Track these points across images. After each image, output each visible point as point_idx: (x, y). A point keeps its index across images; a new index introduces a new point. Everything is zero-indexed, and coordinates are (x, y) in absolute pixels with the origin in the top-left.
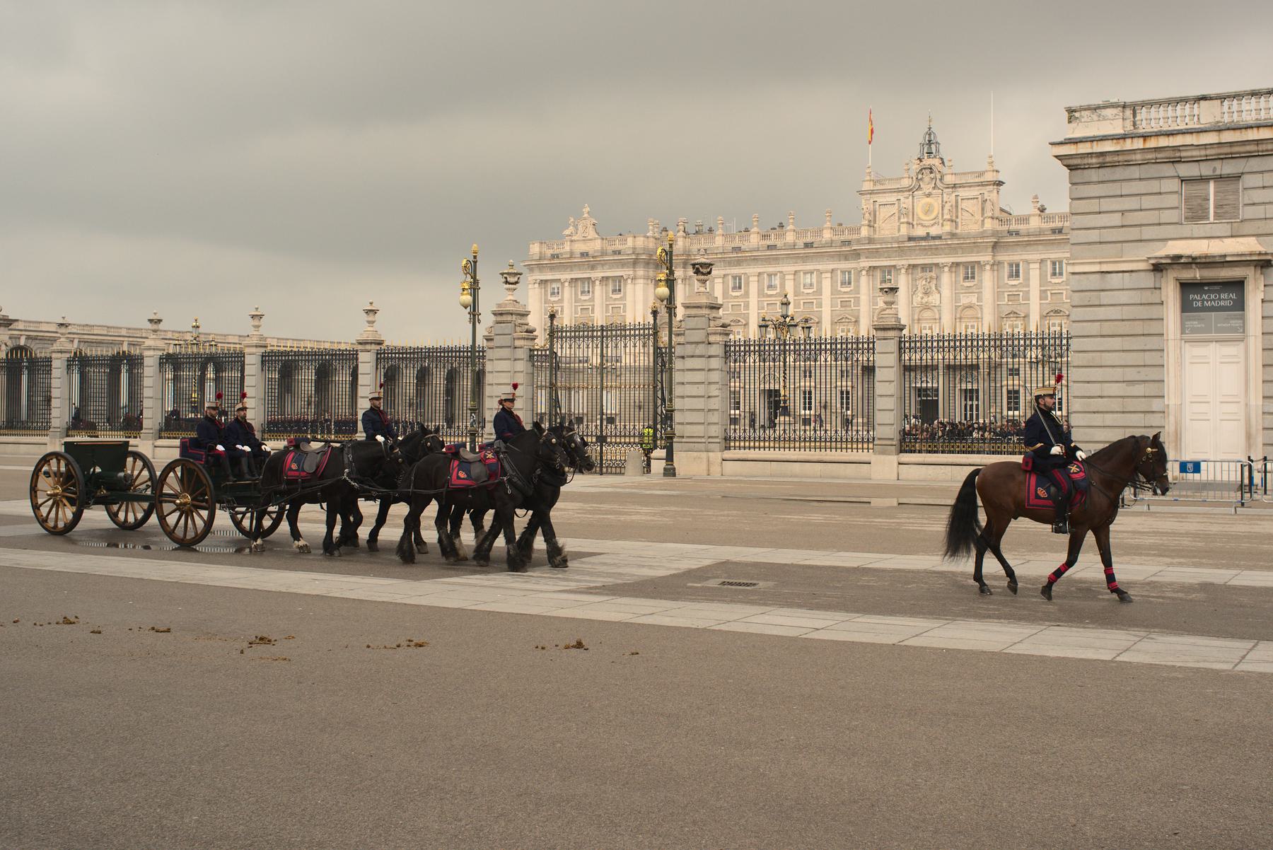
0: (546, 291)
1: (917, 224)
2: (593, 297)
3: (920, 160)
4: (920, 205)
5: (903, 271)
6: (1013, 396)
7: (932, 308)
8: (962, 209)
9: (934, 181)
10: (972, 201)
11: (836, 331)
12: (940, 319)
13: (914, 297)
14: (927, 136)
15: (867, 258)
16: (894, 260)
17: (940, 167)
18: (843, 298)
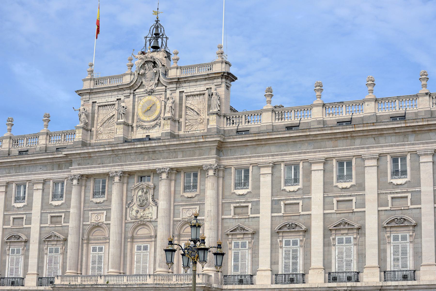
1: (137, 127)
4: (141, 105)
5: (117, 179)
7: (148, 224)
9: (157, 78)
10: (197, 98)
12: (156, 237)
13: (128, 209)
15: (79, 164)
16: (107, 166)
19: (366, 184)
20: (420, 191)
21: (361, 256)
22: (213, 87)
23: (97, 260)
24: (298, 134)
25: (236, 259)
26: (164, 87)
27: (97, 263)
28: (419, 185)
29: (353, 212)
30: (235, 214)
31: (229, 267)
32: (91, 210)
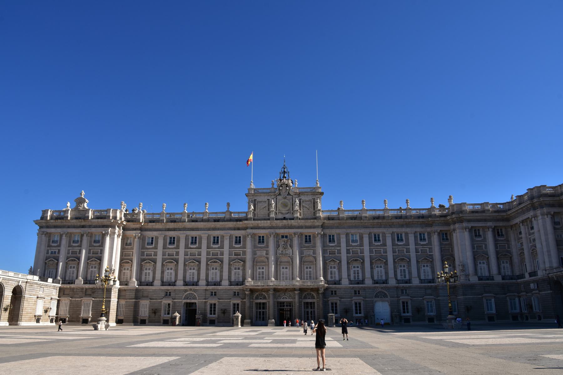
0: (49, 240)
2: (81, 244)
3: (281, 180)
6: (334, 305)
8: (303, 206)
9: (288, 192)
11: (231, 268)
13: (277, 250)
14: (283, 169)
15: (252, 229)
17: (291, 184)
18: (235, 251)
19: (387, 244)
20: (409, 248)
21: (387, 273)
22: (316, 198)
23: (261, 273)
24: (358, 222)
25: (331, 274)
26: (292, 197)
27: (261, 275)
28: (409, 246)
29: (382, 255)
30: (329, 254)
31: (328, 277)
32: (257, 250)
